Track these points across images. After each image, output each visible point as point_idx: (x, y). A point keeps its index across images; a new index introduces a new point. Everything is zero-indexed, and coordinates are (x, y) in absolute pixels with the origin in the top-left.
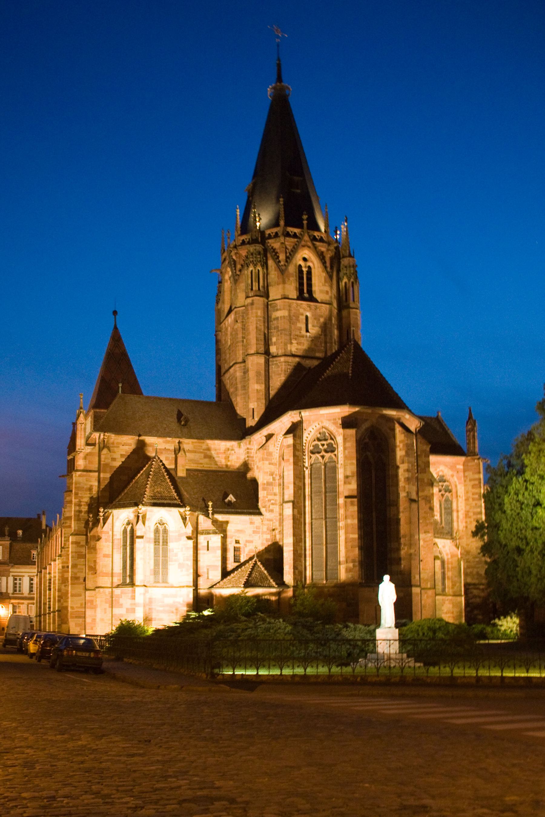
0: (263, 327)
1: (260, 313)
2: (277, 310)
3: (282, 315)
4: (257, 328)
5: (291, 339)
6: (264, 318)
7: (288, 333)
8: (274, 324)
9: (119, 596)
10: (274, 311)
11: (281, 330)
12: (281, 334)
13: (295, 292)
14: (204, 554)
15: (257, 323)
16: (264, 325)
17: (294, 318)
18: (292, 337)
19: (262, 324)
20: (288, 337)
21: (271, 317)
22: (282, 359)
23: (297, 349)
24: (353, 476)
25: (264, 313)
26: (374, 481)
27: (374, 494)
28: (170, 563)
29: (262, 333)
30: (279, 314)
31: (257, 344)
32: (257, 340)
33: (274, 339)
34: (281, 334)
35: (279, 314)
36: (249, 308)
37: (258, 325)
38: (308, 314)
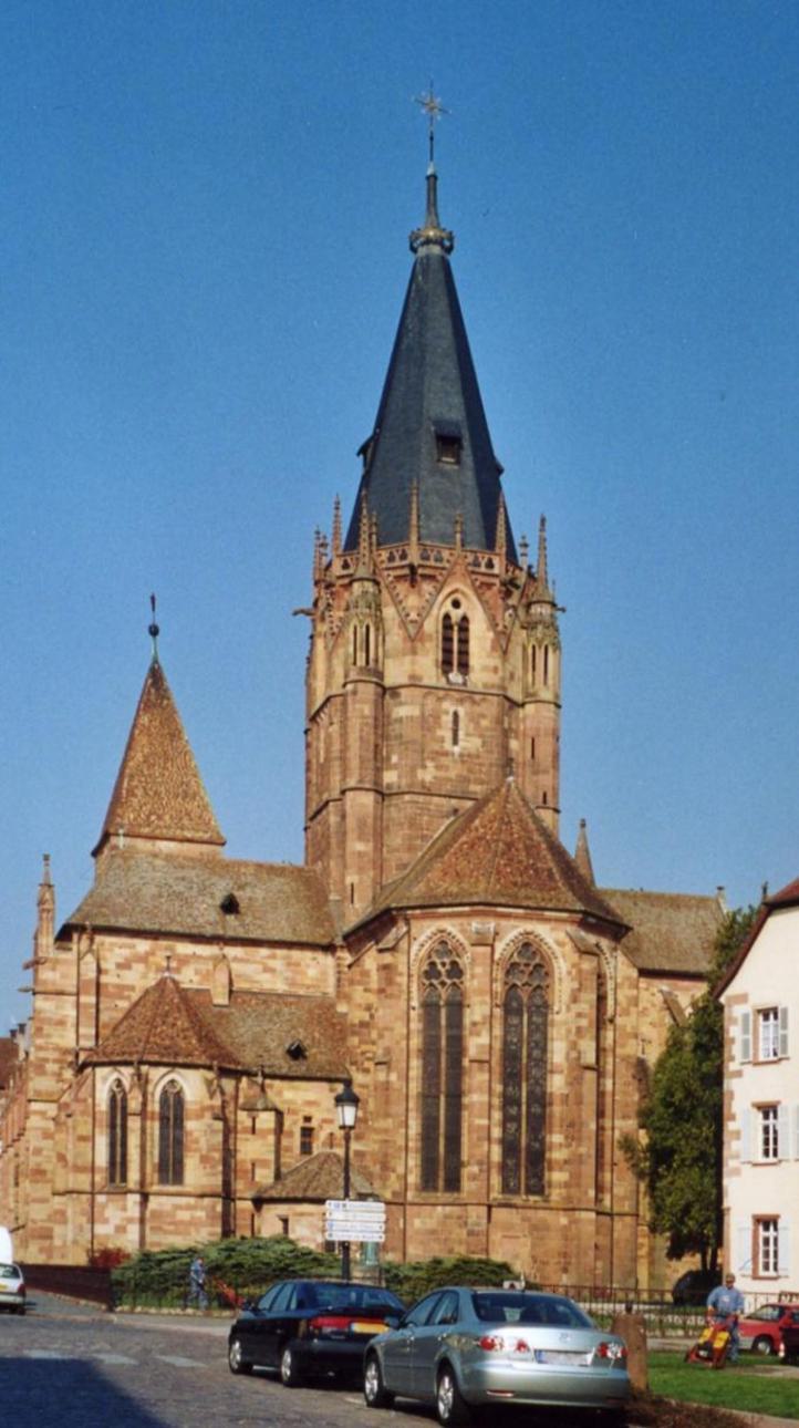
0: (372, 738)
1: (368, 710)
2: (401, 704)
3: (409, 714)
4: (361, 738)
5: (423, 760)
6: (376, 719)
7: (417, 747)
8: (395, 729)
9: (104, 1206)
10: (396, 705)
11: (408, 742)
12: (407, 749)
13: (434, 669)
14: (247, 1140)
15: (361, 730)
16: (376, 733)
17: (431, 719)
18: (426, 755)
19: (372, 731)
21: (389, 716)
22: (407, 797)
23: (435, 778)
24: (484, 1023)
25: (376, 709)
26: (525, 1030)
28: (189, 1154)
29: (372, 748)
31: (361, 768)
32: (362, 761)
33: (394, 759)
34: (407, 749)
35: (401, 711)
36: (350, 699)
37: (364, 734)
38: (462, 711)
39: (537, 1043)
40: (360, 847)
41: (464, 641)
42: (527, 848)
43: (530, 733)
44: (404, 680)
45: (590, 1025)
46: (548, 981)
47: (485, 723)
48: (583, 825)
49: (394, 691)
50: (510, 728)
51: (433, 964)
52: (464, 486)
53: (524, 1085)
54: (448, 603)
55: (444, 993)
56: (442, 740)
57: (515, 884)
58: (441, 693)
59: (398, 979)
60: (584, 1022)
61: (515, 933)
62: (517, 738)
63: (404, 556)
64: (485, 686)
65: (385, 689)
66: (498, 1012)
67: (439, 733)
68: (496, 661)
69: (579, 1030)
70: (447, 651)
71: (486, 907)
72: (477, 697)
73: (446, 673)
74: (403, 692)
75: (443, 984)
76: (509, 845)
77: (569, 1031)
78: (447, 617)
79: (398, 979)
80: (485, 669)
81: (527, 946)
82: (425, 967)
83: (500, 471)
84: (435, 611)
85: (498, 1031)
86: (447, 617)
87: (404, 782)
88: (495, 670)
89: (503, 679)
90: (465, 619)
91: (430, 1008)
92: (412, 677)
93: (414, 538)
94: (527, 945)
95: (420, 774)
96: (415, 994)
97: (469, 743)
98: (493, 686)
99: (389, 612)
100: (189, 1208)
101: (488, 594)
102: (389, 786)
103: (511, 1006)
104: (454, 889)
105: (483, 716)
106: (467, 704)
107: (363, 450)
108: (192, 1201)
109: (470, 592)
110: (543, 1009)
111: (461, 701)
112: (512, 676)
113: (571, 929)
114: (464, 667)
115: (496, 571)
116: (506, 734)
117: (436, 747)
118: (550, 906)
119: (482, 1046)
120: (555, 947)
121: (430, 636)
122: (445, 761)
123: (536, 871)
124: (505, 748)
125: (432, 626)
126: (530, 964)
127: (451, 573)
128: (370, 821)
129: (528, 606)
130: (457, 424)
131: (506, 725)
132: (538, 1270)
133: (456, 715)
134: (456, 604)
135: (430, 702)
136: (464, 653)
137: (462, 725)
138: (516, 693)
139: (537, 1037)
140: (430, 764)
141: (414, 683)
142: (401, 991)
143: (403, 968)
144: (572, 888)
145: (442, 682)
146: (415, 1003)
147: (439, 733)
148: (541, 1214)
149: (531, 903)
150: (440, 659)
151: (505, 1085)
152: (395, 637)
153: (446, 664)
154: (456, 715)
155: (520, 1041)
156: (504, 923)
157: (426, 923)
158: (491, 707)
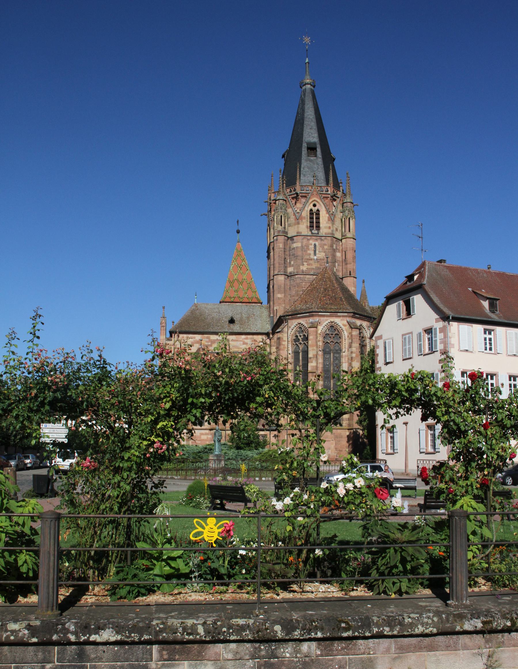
1: (281, 246)
5: (303, 262)
20: (301, 261)
27: (332, 369)
30: (295, 245)
32: (279, 264)
33: (292, 263)
35: (295, 245)
38: (317, 243)
39: (336, 364)
40: (279, 296)
41: (318, 218)
42: (333, 291)
43: (344, 250)
44: (295, 234)
45: (357, 356)
46: (341, 340)
47: (326, 247)
48: (364, 282)
49: (292, 238)
50: (336, 248)
51: (297, 336)
52: (317, 164)
53: (332, 381)
54: (312, 205)
55: (301, 347)
56: (310, 254)
57: (327, 304)
58: (309, 237)
59: (283, 343)
60: (354, 355)
61: (325, 324)
62: (339, 252)
63: (295, 190)
64: (326, 234)
65: (288, 238)
66: (320, 353)
67: (309, 252)
68: (330, 225)
69: (352, 358)
70: (312, 222)
71: (311, 313)
72: (323, 238)
73: (311, 230)
74: (295, 238)
75: (301, 344)
76: (325, 290)
77: (348, 359)
78: (311, 210)
79: (283, 343)
80: (325, 227)
81: (332, 327)
82: (294, 338)
83: (334, 159)
84: (306, 208)
85: (320, 360)
86: (311, 210)
87: (295, 271)
88: (330, 228)
89: (333, 231)
90: (318, 210)
91: (296, 353)
92: (298, 233)
93: (298, 183)
94: (332, 326)
95: (302, 268)
96: (290, 348)
97: (321, 255)
98: (329, 234)
99: (290, 210)
100: (206, 434)
101: (327, 201)
102: (290, 273)
103: (326, 352)
104: (304, 307)
105: (325, 245)
106: (319, 241)
107: (283, 156)
108: (207, 431)
109: (318, 200)
110: (339, 351)
111: (317, 240)
112: (337, 230)
113: (349, 319)
114: (318, 227)
115: (329, 192)
116: (334, 251)
117: (308, 257)
118: (340, 311)
119: (313, 366)
120: (342, 326)
121: (304, 218)
122: (311, 262)
123: (335, 299)
124: (334, 256)
125: (306, 213)
126: (334, 332)
127: (312, 195)
128: (283, 286)
129: (343, 203)
130: (315, 143)
131: (335, 247)
132: (338, 453)
133: (315, 245)
134: (315, 205)
135: (305, 241)
136: (318, 223)
137: (317, 248)
138: (338, 235)
139: (337, 362)
140: (305, 264)
141: (299, 235)
142: (284, 348)
143: (285, 339)
144: (350, 304)
145: (310, 234)
146: (290, 352)
147: (309, 252)
148: (339, 431)
149: (332, 310)
150: (309, 225)
151: (324, 382)
152: (292, 219)
153: (311, 227)
154: (315, 245)
155: (330, 364)
156: (322, 318)
157: (294, 321)
158: (328, 241)
